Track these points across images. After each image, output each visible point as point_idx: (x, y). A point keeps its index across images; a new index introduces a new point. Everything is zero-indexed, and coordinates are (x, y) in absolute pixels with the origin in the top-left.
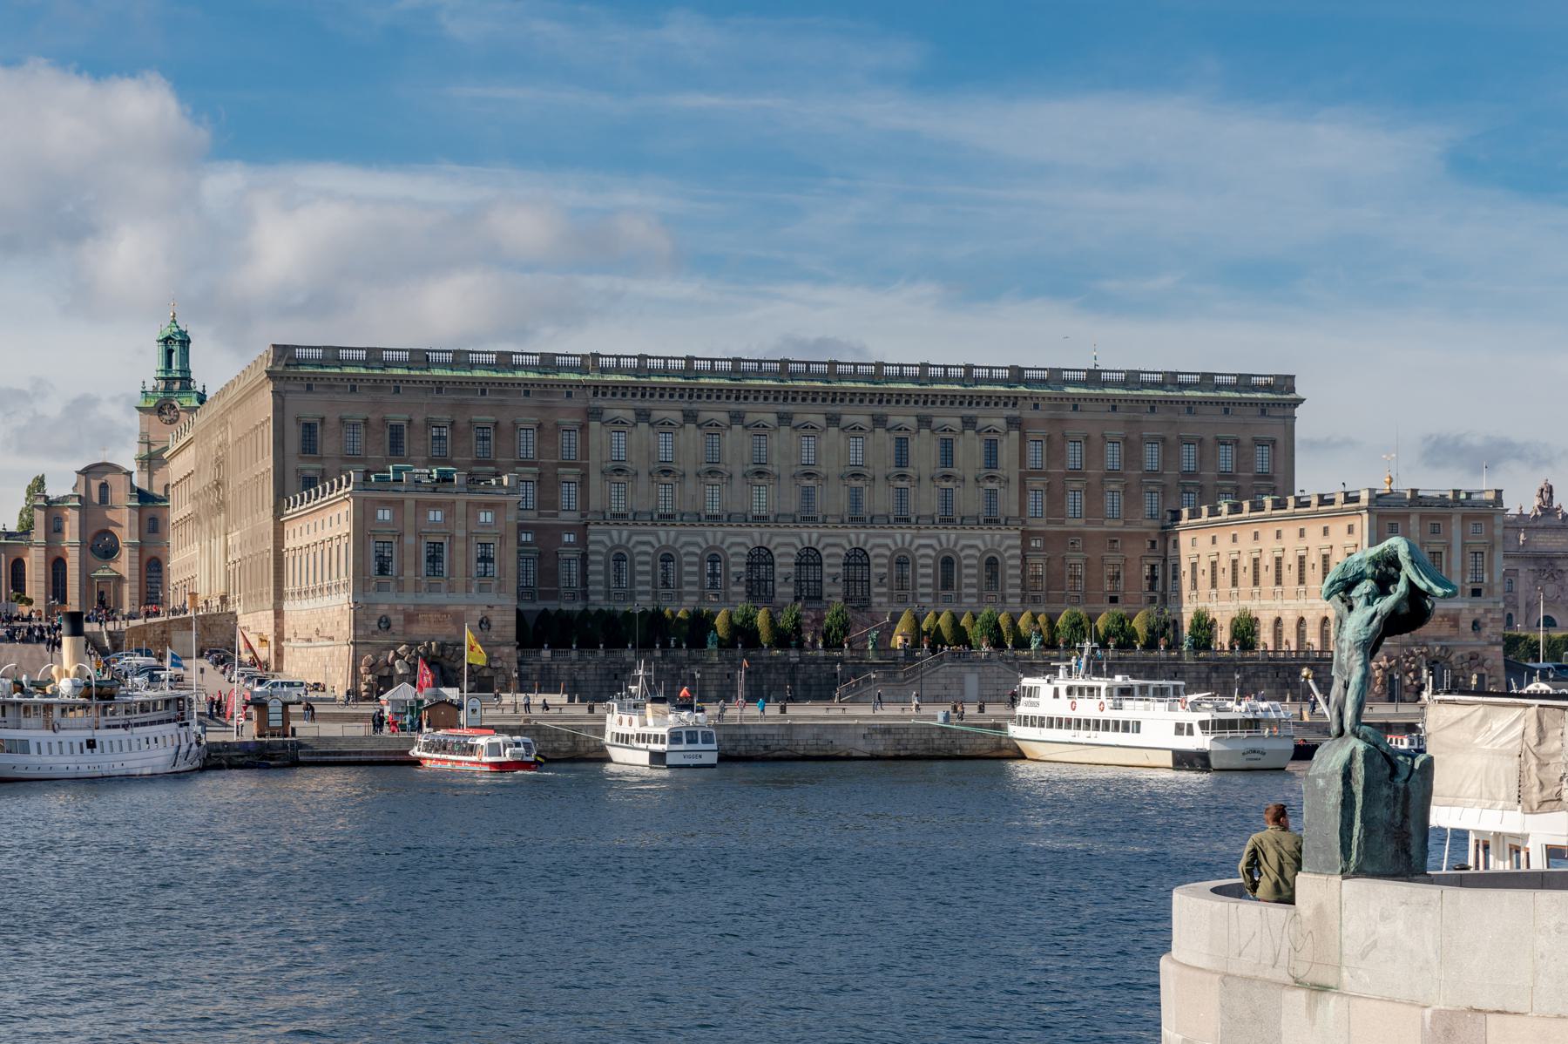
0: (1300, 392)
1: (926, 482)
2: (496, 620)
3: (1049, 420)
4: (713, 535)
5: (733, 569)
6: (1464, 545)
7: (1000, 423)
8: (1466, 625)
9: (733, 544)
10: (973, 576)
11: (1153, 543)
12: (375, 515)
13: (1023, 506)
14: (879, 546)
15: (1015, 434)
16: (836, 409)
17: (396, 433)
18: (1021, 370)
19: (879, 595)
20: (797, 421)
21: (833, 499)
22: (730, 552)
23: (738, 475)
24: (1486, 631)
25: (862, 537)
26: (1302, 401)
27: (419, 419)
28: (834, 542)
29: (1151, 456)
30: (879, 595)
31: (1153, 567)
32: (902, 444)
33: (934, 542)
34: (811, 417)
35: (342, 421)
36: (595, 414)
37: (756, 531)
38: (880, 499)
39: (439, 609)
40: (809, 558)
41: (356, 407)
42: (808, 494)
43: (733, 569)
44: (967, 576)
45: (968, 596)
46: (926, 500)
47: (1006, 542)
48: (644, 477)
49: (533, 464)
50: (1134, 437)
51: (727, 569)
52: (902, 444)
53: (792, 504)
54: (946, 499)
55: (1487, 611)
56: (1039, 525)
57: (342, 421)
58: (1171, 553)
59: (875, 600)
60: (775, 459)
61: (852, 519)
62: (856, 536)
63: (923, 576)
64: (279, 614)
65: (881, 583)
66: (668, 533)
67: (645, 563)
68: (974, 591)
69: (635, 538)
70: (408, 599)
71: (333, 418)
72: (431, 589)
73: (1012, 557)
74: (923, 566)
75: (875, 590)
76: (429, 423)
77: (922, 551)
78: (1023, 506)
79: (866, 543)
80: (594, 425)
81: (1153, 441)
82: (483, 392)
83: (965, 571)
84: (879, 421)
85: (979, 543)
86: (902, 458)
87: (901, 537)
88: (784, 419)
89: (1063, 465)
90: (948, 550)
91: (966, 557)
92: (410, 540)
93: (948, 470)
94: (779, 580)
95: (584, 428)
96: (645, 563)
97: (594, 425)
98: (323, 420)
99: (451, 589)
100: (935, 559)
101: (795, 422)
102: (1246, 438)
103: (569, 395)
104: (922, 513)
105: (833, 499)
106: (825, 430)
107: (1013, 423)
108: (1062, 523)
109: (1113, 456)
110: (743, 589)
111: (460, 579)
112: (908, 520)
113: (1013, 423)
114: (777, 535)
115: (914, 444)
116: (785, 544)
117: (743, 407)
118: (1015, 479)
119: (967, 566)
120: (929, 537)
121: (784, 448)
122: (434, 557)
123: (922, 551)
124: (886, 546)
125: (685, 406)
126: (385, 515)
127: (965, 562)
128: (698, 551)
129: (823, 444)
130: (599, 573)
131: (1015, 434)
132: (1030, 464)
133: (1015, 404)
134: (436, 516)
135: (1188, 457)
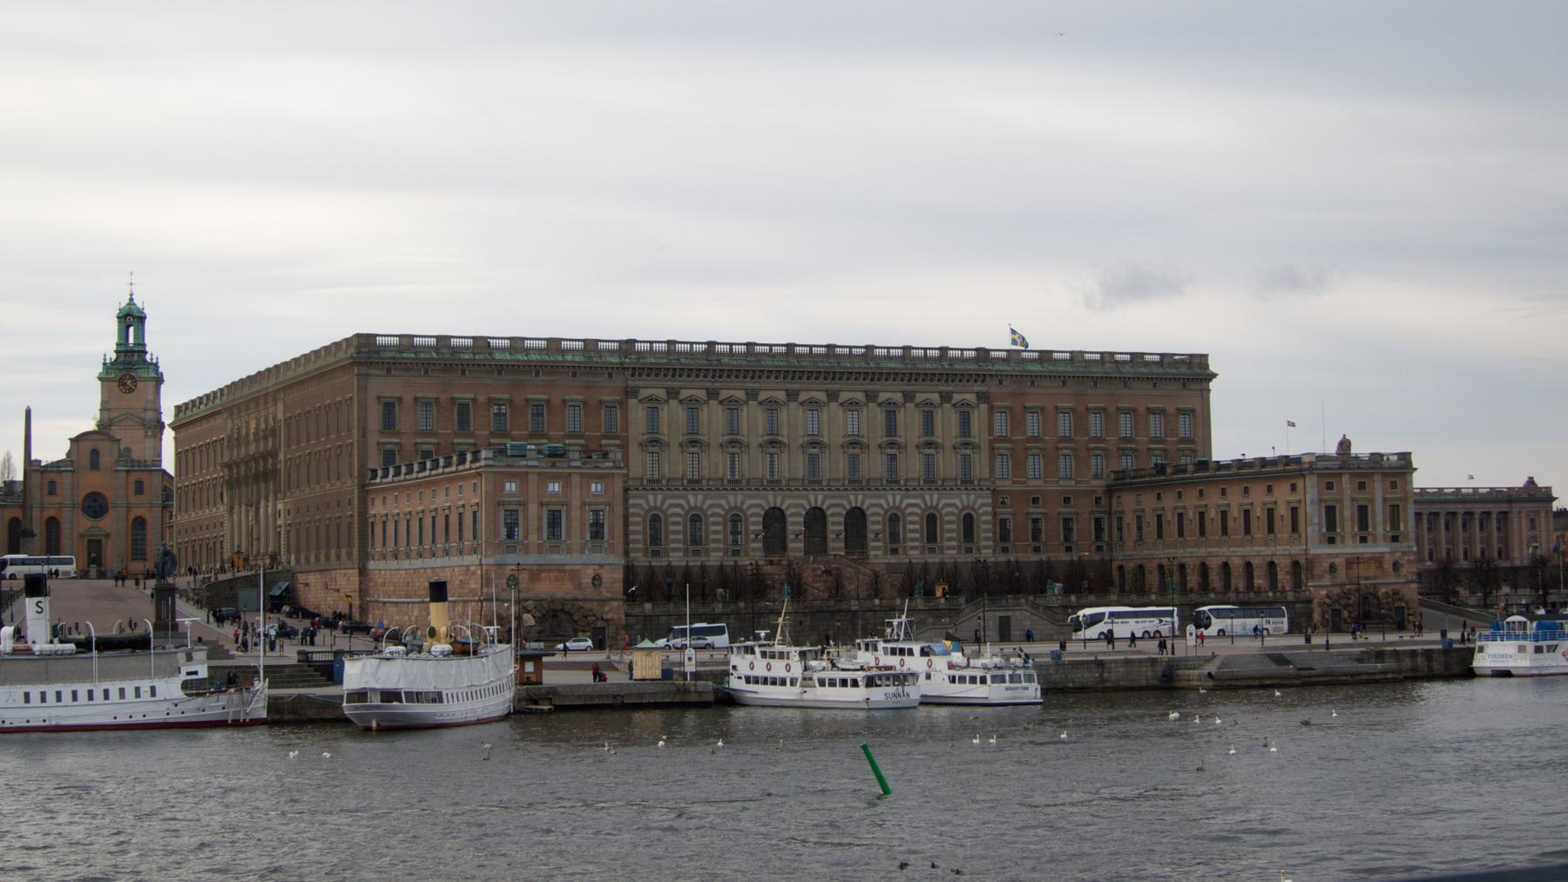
0: (1213, 368)
2: (606, 576)
4: (735, 499)
6: (1385, 500)
7: (971, 398)
8: (1388, 566)
9: (752, 506)
11: (1098, 500)
12: (503, 488)
15: (984, 407)
16: (834, 387)
17: (464, 409)
18: (988, 351)
19: (876, 548)
20: (803, 396)
21: (835, 465)
23: (754, 445)
24: (1404, 571)
26: (1215, 375)
27: (482, 398)
28: (836, 507)
29: (1095, 424)
30: (876, 548)
31: (1098, 521)
32: (891, 418)
34: (815, 394)
35: (416, 399)
36: (630, 392)
37: (770, 495)
38: (874, 465)
39: (559, 568)
40: (816, 518)
41: (428, 388)
42: (813, 460)
45: (949, 548)
46: (912, 465)
47: (982, 504)
48: (675, 449)
49: (580, 437)
50: (1081, 408)
52: (891, 418)
53: (800, 469)
54: (929, 465)
55: (1404, 553)
56: (1006, 485)
57: (416, 399)
58: (1114, 508)
59: (873, 553)
60: (784, 430)
62: (856, 499)
64: (363, 572)
65: (876, 539)
67: (677, 523)
68: (954, 543)
69: (668, 502)
70: (532, 559)
71: (408, 399)
72: (555, 549)
73: (985, 514)
76: (490, 401)
78: (992, 469)
80: (632, 402)
81: (1097, 411)
82: (537, 374)
83: (947, 527)
84: (871, 396)
85: (957, 502)
86: (891, 428)
87: (893, 498)
88: (792, 395)
89: (1025, 432)
92: (533, 508)
94: (791, 537)
95: (623, 404)
96: (677, 523)
97: (632, 402)
98: (400, 399)
99: (569, 551)
100: (921, 516)
102: (1171, 410)
103: (610, 375)
104: (911, 476)
105: (835, 465)
106: (746, 403)
107: (983, 397)
109: (1064, 425)
110: (760, 545)
111: (576, 541)
112: (897, 482)
113: (983, 397)
115: (900, 416)
116: (795, 507)
117: (676, 384)
118: (985, 446)
120: (916, 497)
121: (795, 422)
122: (554, 520)
124: (880, 505)
126: (511, 487)
129: (825, 416)
130: (638, 533)
131: (984, 407)
132: (997, 433)
134: (555, 487)
135: (1125, 425)
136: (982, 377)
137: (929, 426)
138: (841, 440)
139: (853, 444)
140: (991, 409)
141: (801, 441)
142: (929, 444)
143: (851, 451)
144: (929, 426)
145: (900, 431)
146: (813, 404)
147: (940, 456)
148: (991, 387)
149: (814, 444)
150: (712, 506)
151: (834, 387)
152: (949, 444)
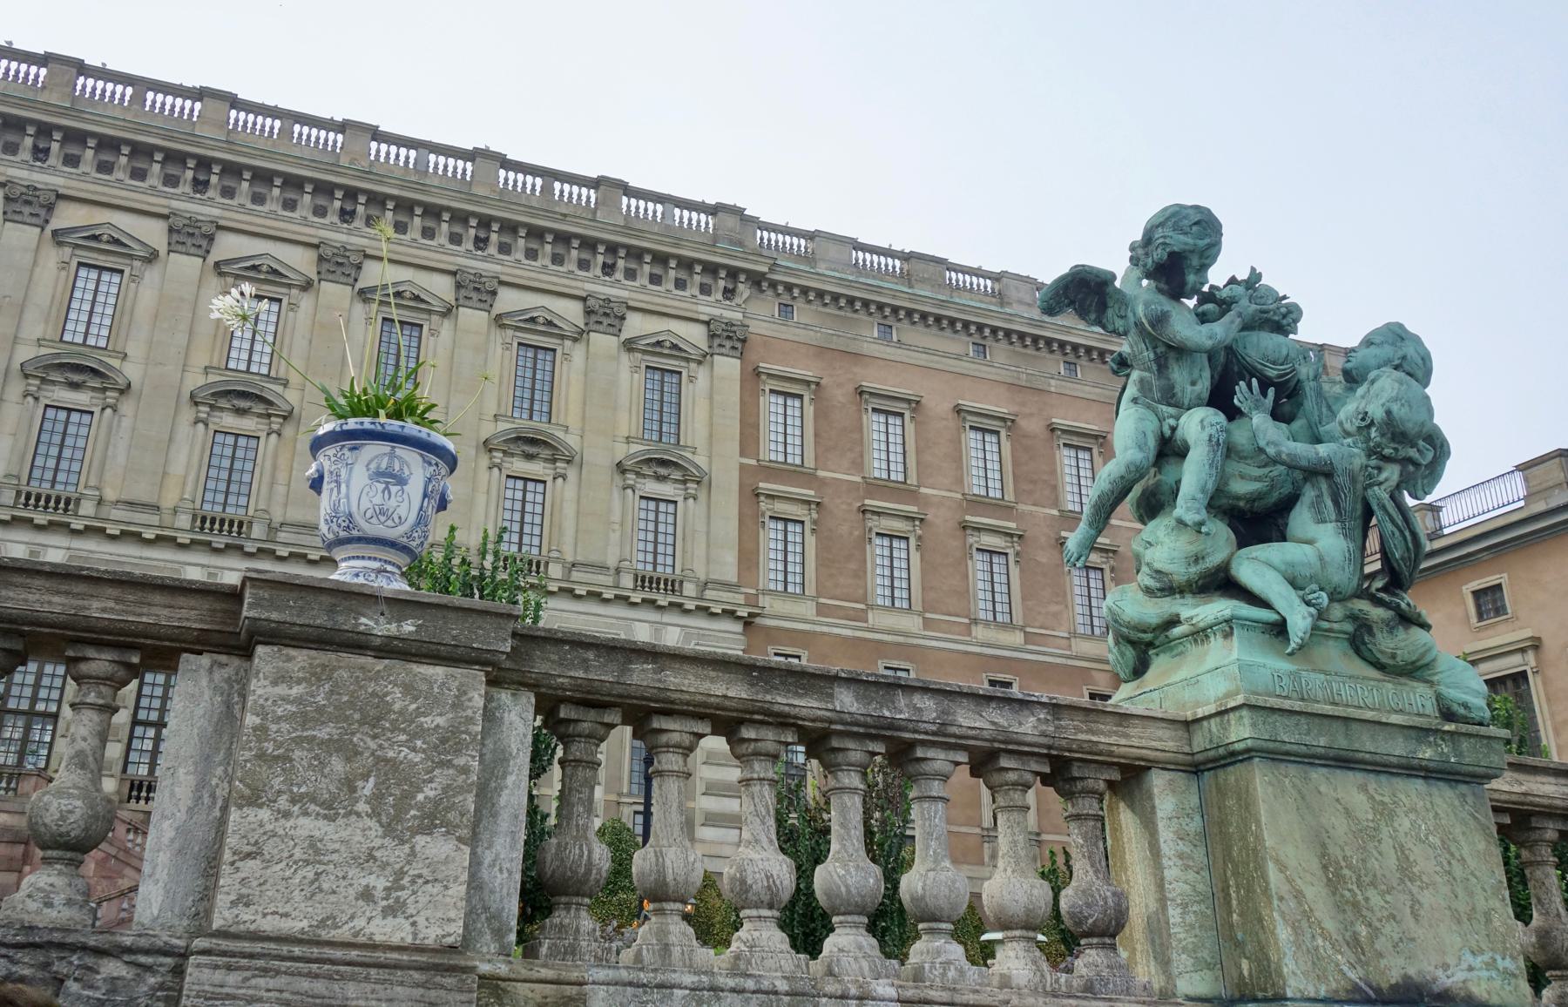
3: (822, 351)
13: (748, 558)
78: (748, 558)
84: (339, 265)
89: (859, 464)
93: (538, 424)
101: (57, 223)
108: (860, 616)
131: (728, 367)
132: (771, 452)
133: (729, 293)
136: (730, 277)
138: (195, 380)
140: (753, 376)
141: (25, 353)
142: (531, 444)
143: (229, 421)
148: (757, 314)
151: (206, 209)
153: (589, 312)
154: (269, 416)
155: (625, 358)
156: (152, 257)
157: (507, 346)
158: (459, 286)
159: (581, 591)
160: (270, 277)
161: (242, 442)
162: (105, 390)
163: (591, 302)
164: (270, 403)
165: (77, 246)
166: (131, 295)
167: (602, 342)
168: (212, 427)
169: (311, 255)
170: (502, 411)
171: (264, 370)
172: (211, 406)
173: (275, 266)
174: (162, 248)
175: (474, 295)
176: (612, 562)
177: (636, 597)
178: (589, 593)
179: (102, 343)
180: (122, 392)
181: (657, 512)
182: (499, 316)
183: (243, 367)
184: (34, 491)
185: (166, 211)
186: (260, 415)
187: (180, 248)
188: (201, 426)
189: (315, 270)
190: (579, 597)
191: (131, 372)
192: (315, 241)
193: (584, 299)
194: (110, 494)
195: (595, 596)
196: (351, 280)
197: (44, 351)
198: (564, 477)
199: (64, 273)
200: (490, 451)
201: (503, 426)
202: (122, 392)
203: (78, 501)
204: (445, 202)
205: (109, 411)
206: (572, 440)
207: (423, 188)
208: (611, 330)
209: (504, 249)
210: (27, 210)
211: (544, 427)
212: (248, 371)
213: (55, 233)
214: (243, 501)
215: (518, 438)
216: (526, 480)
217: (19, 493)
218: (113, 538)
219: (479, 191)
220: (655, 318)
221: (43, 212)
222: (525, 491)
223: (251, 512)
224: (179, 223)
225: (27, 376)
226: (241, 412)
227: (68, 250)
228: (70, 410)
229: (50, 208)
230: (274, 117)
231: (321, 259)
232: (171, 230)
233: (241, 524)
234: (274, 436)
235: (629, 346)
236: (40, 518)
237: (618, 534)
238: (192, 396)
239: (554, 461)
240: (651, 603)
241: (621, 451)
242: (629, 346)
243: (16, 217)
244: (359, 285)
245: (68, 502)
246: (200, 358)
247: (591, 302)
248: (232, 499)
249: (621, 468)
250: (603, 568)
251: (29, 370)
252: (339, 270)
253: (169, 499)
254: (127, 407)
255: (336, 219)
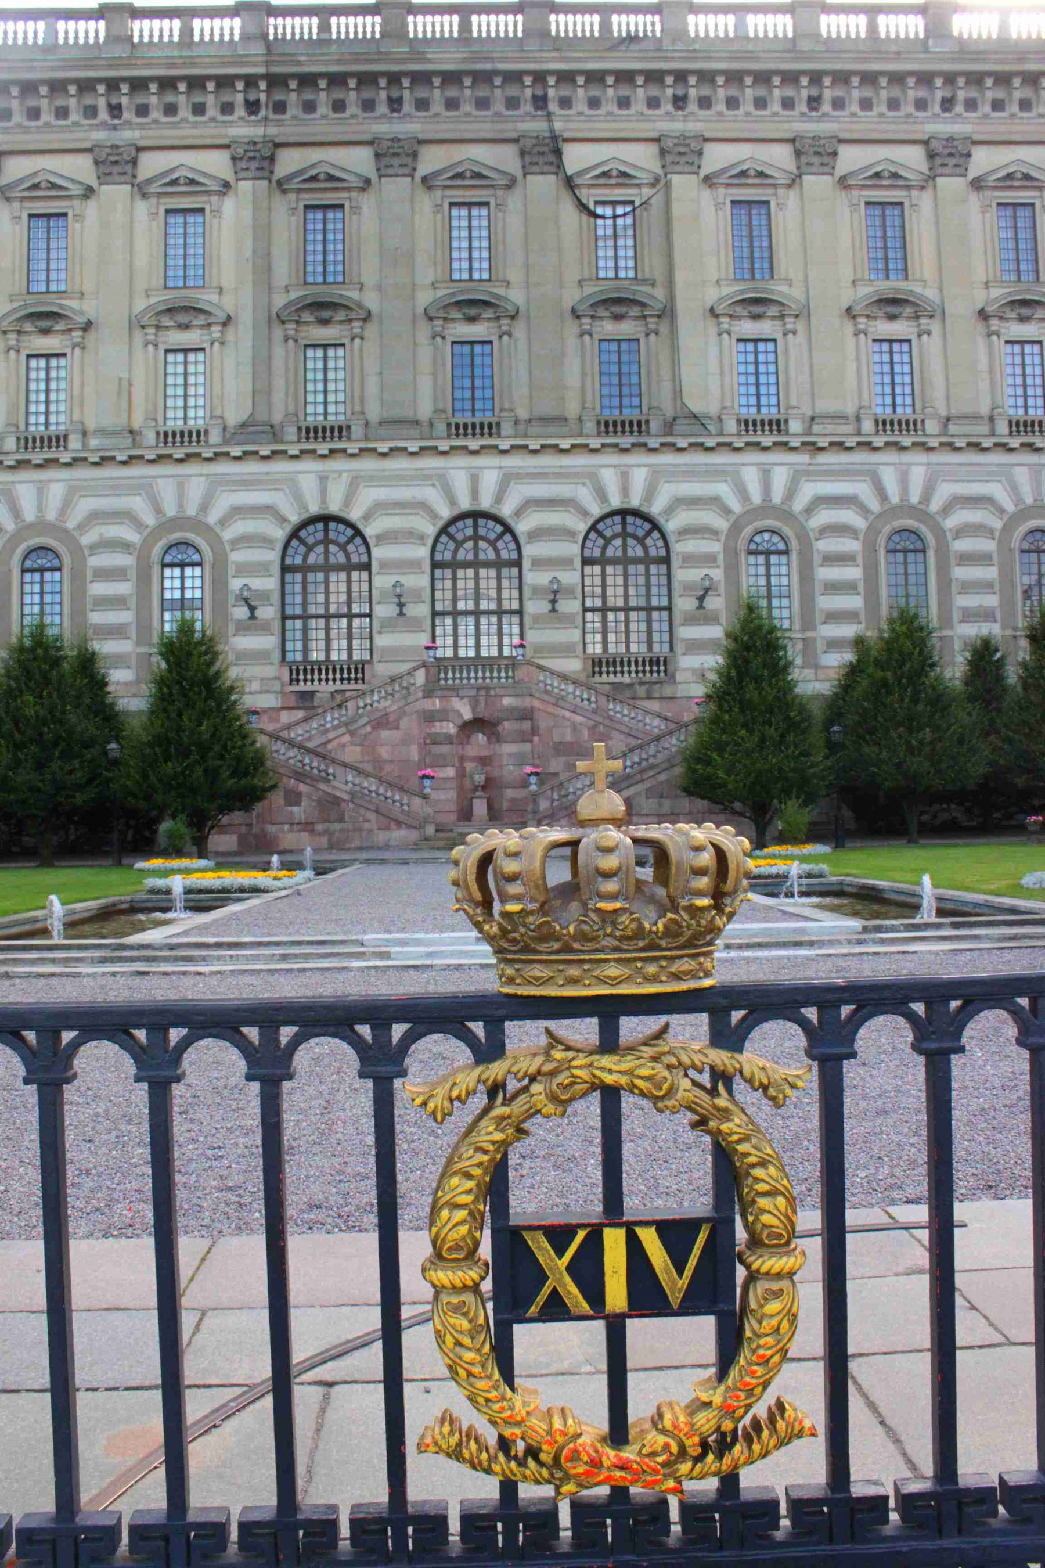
1: (827, 319)
5: (236, 584)
9: (237, 512)
10: (987, 586)
14: (694, 502)
22: (227, 535)
25: (639, 477)
32: (751, 212)
33: (862, 489)
34: (481, 154)
43: (236, 584)
44: (967, 587)
51: (219, 583)
61: (607, 427)
63: (834, 587)
66: (41, 490)
74: (831, 559)
75: (686, 633)
77: (824, 517)
79: (650, 493)
83: (961, 573)
85: (997, 490)
87: (762, 477)
90: (906, 508)
91: (960, 532)
104: (823, 406)
114: (373, 479)
115: (788, 215)
119: (967, 559)
123: (824, 517)
124: (715, 502)
125: (100, 136)
127: (961, 545)
128: (133, 536)
129: (513, 221)
137: (890, 247)
138: (571, 296)
139: (616, 304)
141: (424, 298)
142: (892, 305)
143: (609, 328)
144: (890, 247)
145: (787, 262)
146: (469, 188)
147: (932, 344)
149: (473, 307)
150: (96, 517)
152: (962, 305)
153: (931, 156)
154: (645, 317)
155: (973, 198)
156: (511, 184)
157: (853, 206)
158: (798, 154)
159: (960, 443)
160: (620, 181)
161: (624, 346)
162: (498, 318)
163: (934, 144)
164: (643, 305)
165: (446, 187)
166: (500, 224)
167: (950, 185)
168: (596, 337)
169: (653, 149)
170: (859, 275)
171: (631, 274)
172: (592, 317)
173: (623, 168)
174: (519, 174)
175: (816, 160)
176: (984, 410)
177: (1015, 443)
178: (969, 444)
179: (485, 276)
180: (513, 318)
181: (1023, 354)
182: (843, 178)
183: (611, 274)
184: (461, 421)
185: (514, 135)
186: (637, 318)
187: (534, 168)
188: (587, 337)
189: (659, 164)
190: (960, 449)
191: (516, 296)
192: (655, 135)
193: (926, 143)
194: (523, 413)
195: (975, 446)
196: (695, 169)
197: (440, 293)
198: (929, 333)
199: (439, 216)
200: (854, 317)
201: (864, 291)
202: (513, 318)
203: (498, 424)
204: (772, 66)
205: (505, 338)
206: (931, 293)
207: (750, 56)
208: (958, 170)
209: (838, 104)
210: (396, 162)
211: (903, 285)
212: (617, 278)
213: (424, 179)
214: (636, 401)
215: (880, 301)
216: (891, 341)
217: (449, 425)
218: (535, 452)
219: (805, 45)
220: (1002, 149)
221: (409, 160)
222: (891, 353)
223: (645, 410)
224: (528, 143)
225: (431, 319)
226: (618, 318)
227: (439, 193)
228: (472, 343)
229: (415, 155)
230: (591, 13)
231: (663, 152)
232: (522, 154)
233: (639, 423)
234: (653, 336)
235: (977, 184)
236: (474, 444)
237: (987, 382)
238: (573, 311)
239: (917, 318)
240: (1030, 447)
241: (979, 298)
242: (977, 184)
243: (390, 171)
244: (704, 171)
245: (490, 426)
246: (572, 274)
247: (934, 144)
248: (626, 401)
249: (983, 315)
250: (977, 418)
251: (432, 313)
252: (683, 159)
253: (572, 409)
254: (519, 330)
255: (670, 107)
